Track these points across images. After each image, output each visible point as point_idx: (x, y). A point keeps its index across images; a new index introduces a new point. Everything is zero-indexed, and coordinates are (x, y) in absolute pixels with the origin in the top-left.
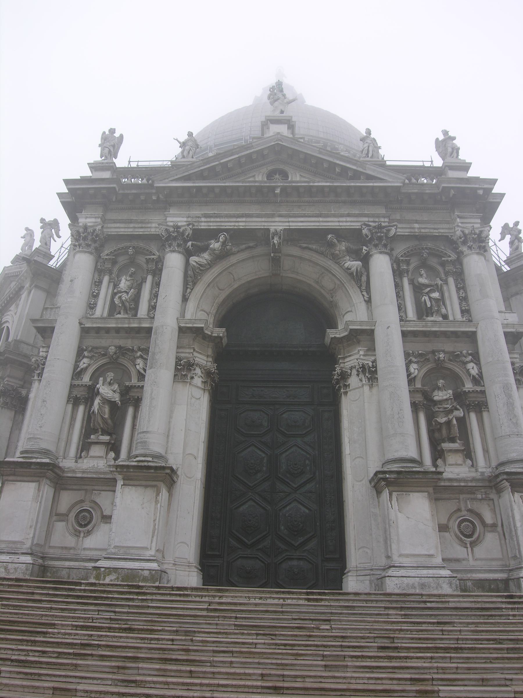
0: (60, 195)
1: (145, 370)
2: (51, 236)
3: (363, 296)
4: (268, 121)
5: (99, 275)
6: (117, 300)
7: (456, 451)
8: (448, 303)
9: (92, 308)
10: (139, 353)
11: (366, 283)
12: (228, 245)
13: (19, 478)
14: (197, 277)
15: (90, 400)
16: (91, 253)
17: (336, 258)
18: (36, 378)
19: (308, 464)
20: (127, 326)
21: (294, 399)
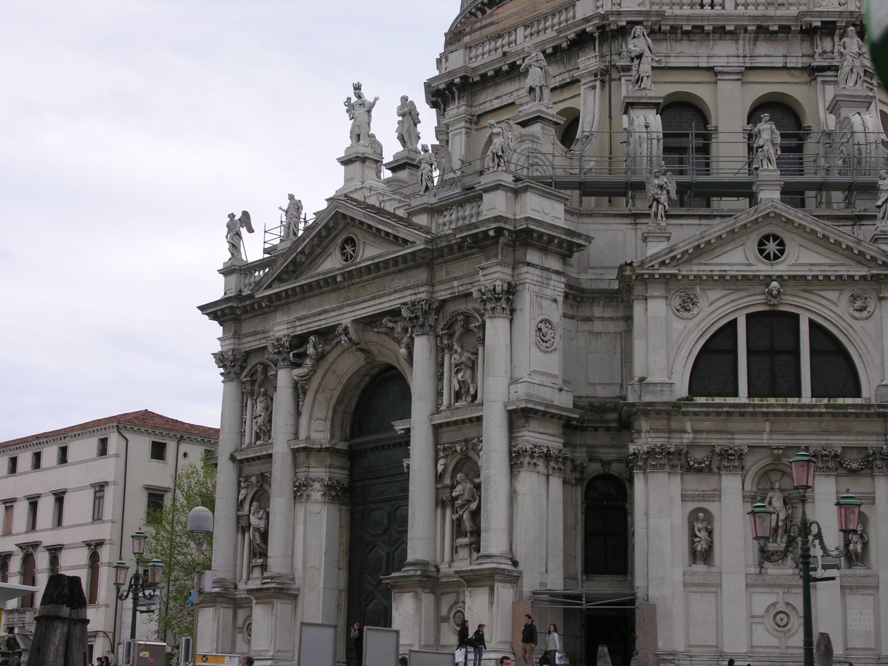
7: (466, 545)
13: (206, 605)
16: (232, 380)
17: (399, 342)
20: (260, 454)
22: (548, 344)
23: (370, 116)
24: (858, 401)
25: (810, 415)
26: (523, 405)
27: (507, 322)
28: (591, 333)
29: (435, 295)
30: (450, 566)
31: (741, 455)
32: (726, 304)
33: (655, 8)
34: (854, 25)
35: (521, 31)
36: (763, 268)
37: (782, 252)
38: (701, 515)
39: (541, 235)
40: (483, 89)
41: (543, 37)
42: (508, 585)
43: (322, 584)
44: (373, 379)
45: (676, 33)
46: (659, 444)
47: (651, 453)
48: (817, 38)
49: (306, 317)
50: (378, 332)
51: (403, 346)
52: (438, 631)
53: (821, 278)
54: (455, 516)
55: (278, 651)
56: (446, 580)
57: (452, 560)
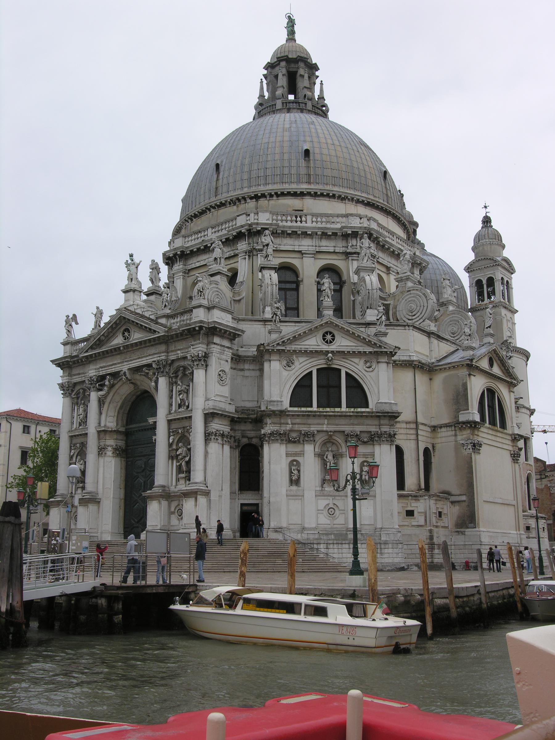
16: (67, 397)
17: (151, 380)
20: (81, 433)
22: (223, 382)
23: (137, 270)
24: (367, 410)
25: (345, 416)
26: (212, 411)
27: (205, 371)
28: (243, 376)
29: (169, 357)
30: (175, 488)
31: (314, 435)
32: (307, 364)
33: (274, 222)
34: (366, 233)
35: (210, 230)
36: (325, 347)
37: (333, 340)
38: (295, 463)
39: (221, 330)
40: (192, 257)
41: (220, 233)
42: (204, 497)
43: (112, 496)
44: (138, 397)
45: (284, 234)
46: (276, 430)
47: (272, 434)
48: (349, 239)
49: (105, 367)
51: (153, 381)
52: (169, 518)
53: (351, 352)
54: (178, 464)
55: (91, 529)
56: (174, 494)
57: (176, 485)
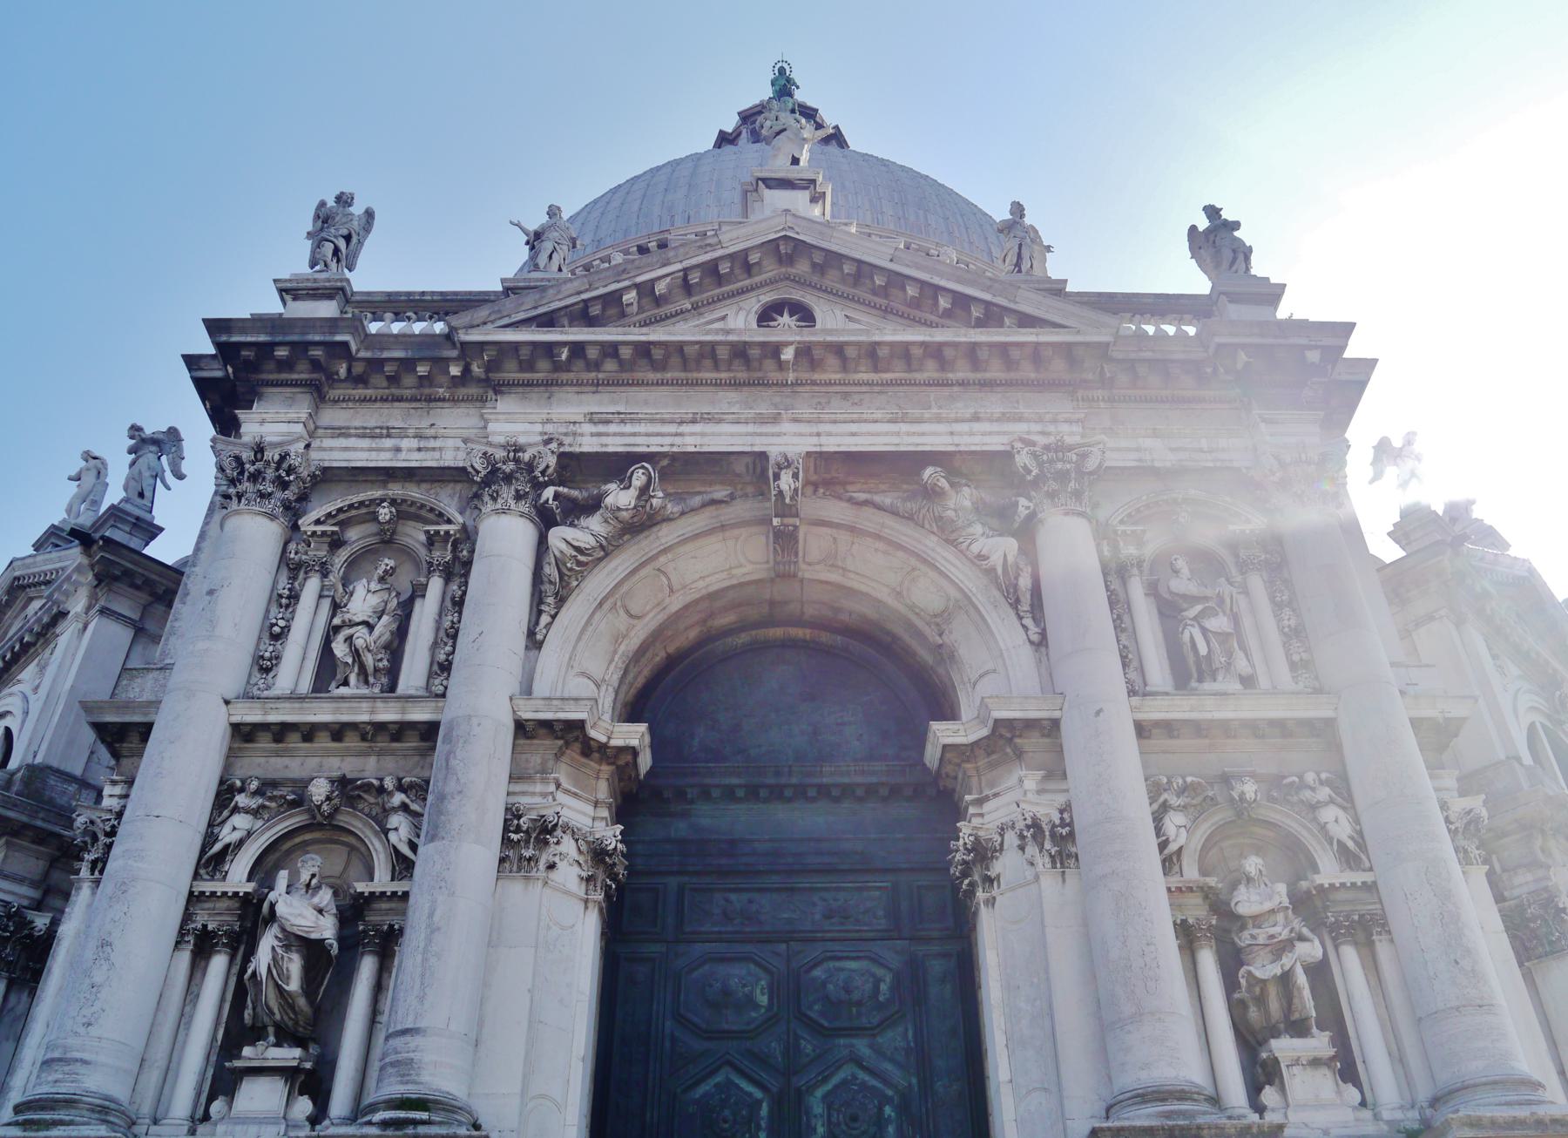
0: (191, 361)
1: (413, 847)
2: (157, 475)
3: (1024, 626)
4: (760, 182)
5: (290, 578)
6: (340, 649)
8: (1252, 643)
9: (267, 670)
10: (399, 798)
11: (1032, 595)
12: (653, 497)
14: (568, 584)
15: (245, 937)
16: (272, 517)
17: (949, 533)
18: (85, 872)
19: (890, 1116)
20: (365, 718)
21: (842, 924)
50: (866, 503)
